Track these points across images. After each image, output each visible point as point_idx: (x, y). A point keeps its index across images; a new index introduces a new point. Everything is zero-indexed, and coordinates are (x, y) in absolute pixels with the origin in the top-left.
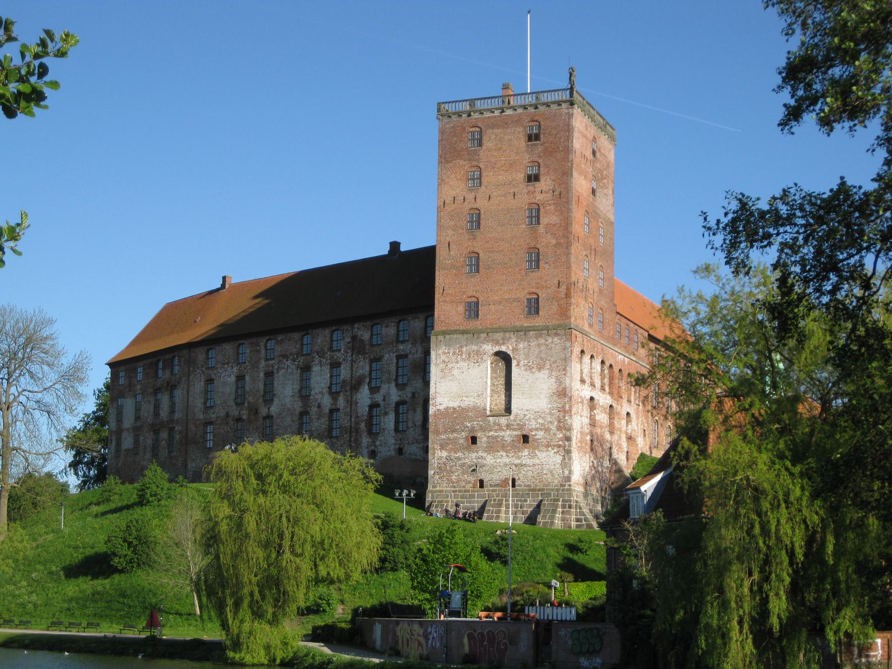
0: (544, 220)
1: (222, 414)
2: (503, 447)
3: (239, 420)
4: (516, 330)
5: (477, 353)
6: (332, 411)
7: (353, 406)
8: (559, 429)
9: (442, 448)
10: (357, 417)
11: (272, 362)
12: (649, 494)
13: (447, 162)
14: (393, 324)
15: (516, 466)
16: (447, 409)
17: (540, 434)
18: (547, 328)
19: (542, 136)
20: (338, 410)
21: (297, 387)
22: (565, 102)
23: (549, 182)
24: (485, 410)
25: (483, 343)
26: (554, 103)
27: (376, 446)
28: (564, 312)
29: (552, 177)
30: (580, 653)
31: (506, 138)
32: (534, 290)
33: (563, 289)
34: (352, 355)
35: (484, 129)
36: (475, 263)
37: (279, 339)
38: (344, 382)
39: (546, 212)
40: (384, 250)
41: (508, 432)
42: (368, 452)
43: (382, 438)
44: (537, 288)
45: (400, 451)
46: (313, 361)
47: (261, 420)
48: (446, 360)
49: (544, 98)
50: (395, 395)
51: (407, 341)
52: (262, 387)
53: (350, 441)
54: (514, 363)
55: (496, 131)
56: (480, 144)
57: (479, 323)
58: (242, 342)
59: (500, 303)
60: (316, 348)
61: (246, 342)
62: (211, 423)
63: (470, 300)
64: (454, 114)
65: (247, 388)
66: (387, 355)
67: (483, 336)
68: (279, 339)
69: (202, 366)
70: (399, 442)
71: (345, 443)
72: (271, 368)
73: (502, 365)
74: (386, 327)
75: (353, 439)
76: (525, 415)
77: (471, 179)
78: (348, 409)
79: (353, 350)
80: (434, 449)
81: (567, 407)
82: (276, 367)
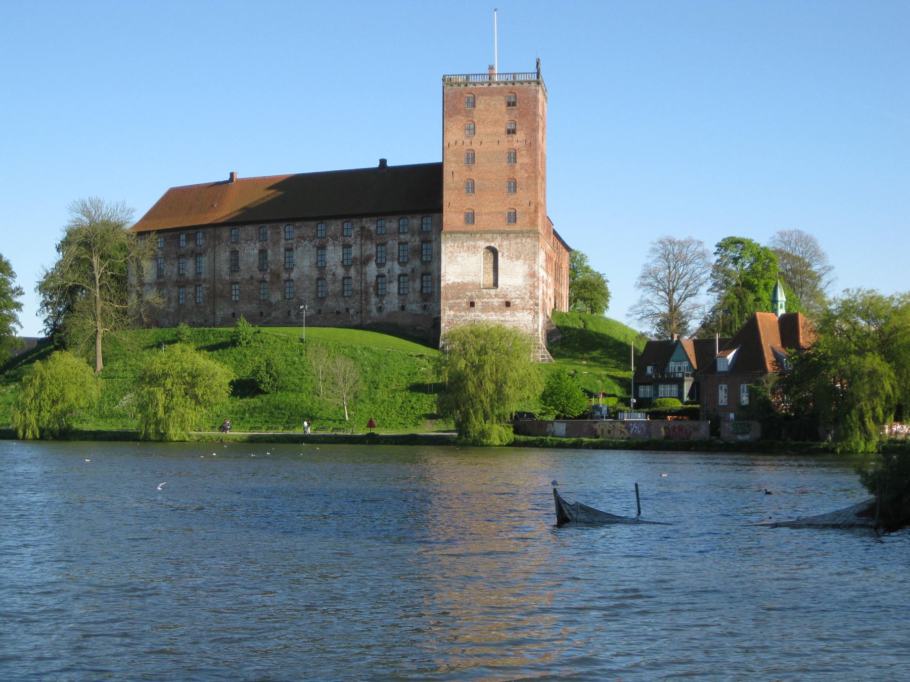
0: (519, 160)
1: (247, 276)
2: (493, 309)
3: (263, 281)
4: (501, 233)
5: (474, 247)
6: (344, 278)
7: (363, 276)
8: (531, 298)
9: (450, 309)
10: (366, 283)
11: (291, 241)
12: (730, 360)
13: (451, 116)
14: (395, 220)
15: (502, 321)
16: (453, 283)
17: (518, 301)
18: (522, 232)
19: (517, 104)
20: (350, 278)
21: (314, 260)
22: (534, 81)
23: (522, 135)
24: (480, 284)
25: (478, 240)
26: (526, 81)
27: (383, 304)
28: (534, 223)
29: (525, 132)
30: (738, 434)
31: (492, 103)
32: (513, 207)
33: (533, 207)
34: (361, 240)
35: (476, 96)
36: (471, 187)
37: (297, 225)
38: (355, 258)
39: (521, 155)
40: (376, 165)
41: (496, 299)
42: (376, 308)
44: (515, 205)
45: (403, 308)
46: (328, 242)
47: (282, 282)
48: (453, 251)
49: (519, 78)
50: (397, 270)
51: (407, 233)
52: (282, 259)
53: (361, 300)
54: (500, 255)
55: (485, 97)
56: (474, 105)
57: (475, 227)
58: (264, 225)
59: (489, 214)
60: (330, 233)
61: (267, 226)
62: (237, 283)
63: (468, 211)
64: (455, 84)
65: (269, 259)
66: (391, 242)
67: (478, 236)
68: (297, 225)
69: (227, 241)
71: (356, 301)
72: (290, 246)
73: (491, 255)
74: (390, 222)
75: (363, 298)
76: (508, 289)
77: (468, 130)
78: (359, 278)
79: (362, 236)
80: (445, 310)
81: (536, 284)
82: (295, 245)
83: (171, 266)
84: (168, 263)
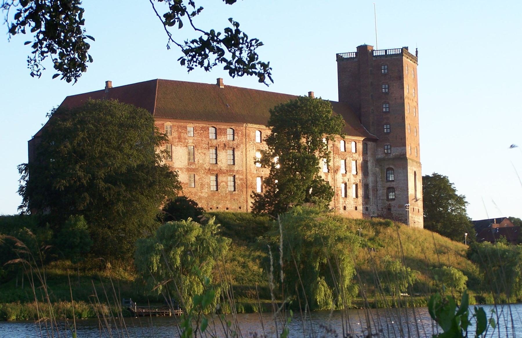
27: (346, 204)
34: (333, 154)
43: (348, 200)
70: (355, 203)
78: (333, 183)
83: (203, 155)
84: (200, 151)
